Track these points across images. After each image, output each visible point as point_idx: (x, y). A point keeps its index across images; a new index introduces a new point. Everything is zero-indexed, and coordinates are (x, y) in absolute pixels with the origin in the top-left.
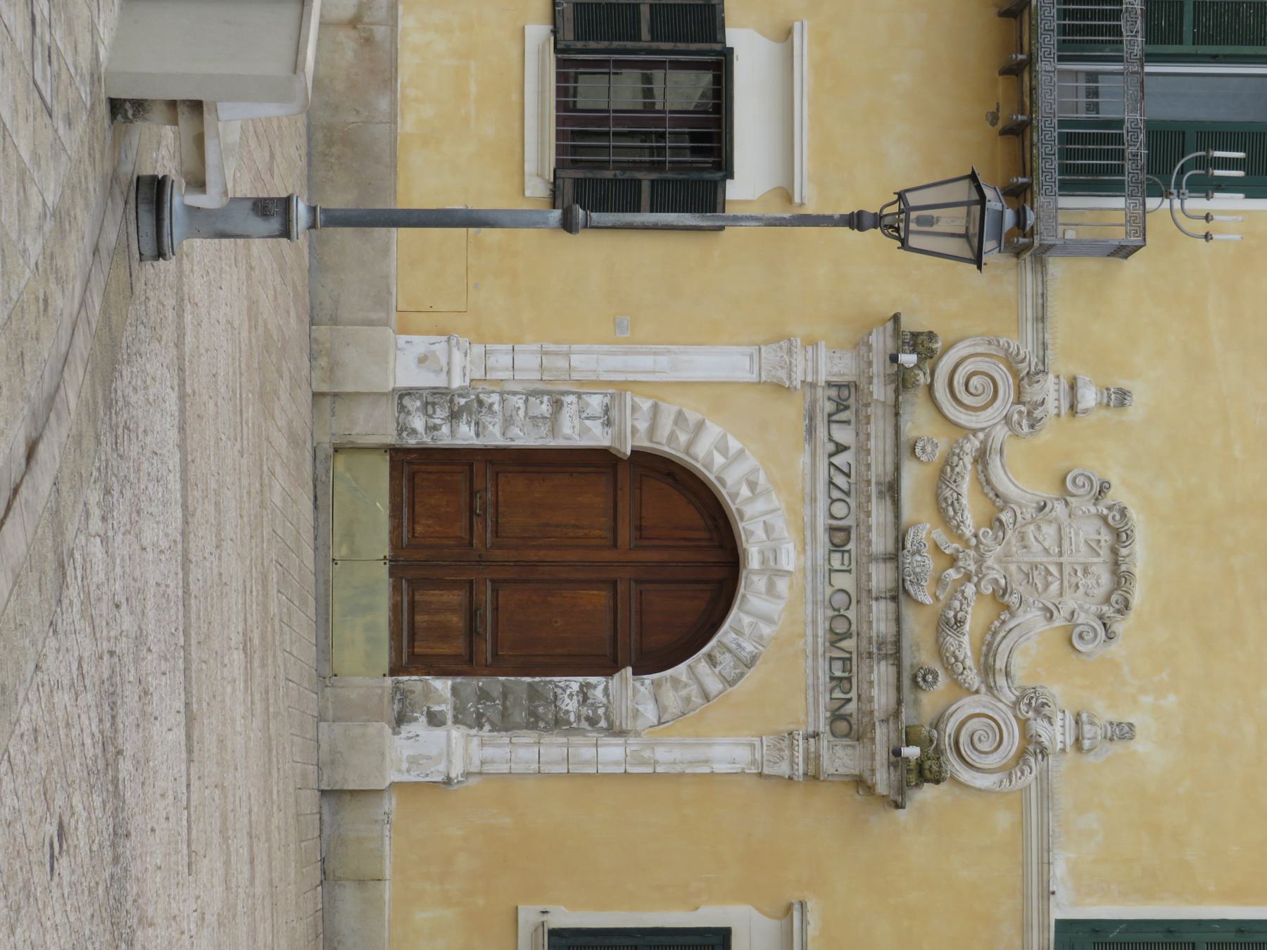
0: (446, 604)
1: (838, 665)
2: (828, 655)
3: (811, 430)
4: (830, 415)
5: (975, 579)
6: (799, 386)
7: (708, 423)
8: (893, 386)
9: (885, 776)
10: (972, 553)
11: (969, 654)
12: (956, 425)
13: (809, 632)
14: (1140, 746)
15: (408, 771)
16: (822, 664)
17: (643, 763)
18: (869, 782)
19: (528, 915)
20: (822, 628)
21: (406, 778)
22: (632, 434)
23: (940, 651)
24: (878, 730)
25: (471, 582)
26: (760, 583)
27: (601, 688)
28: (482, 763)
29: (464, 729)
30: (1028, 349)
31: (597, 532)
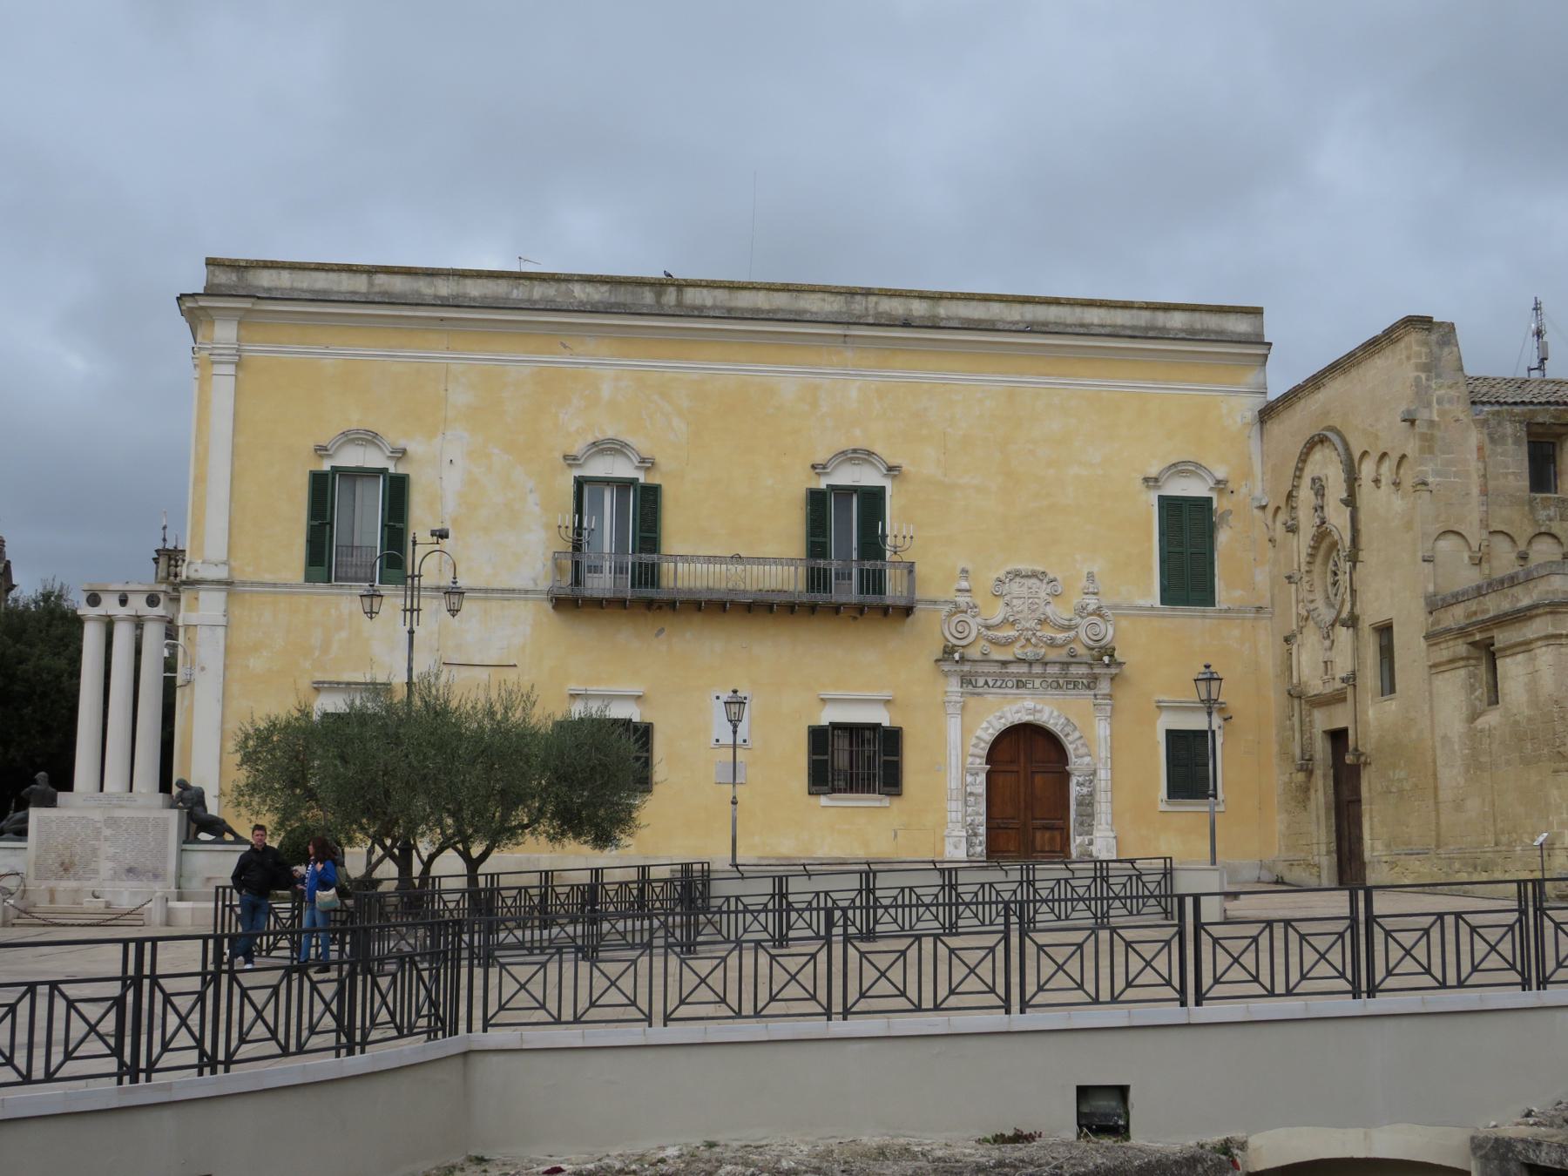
0: (1041, 838)
14: (1095, 569)
19: (1163, 807)
22: (980, 764)
23: (1061, 646)
26: (1038, 716)
30: (947, 608)
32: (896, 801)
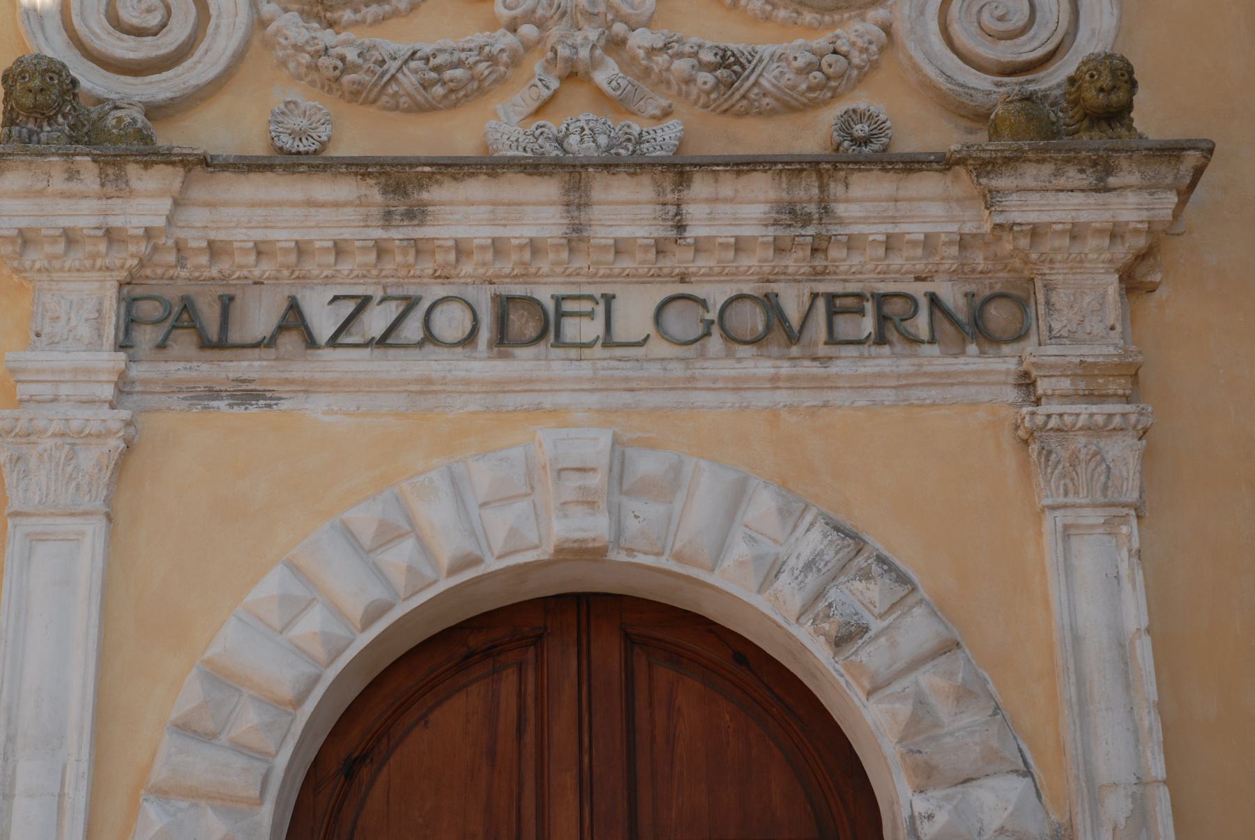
1: (845, 326)
2: (823, 350)
3: (247, 395)
4: (205, 344)
5: (619, 28)
6: (125, 414)
7: (214, 651)
8: (133, 170)
9: (1132, 198)
10: (555, 32)
11: (800, 41)
12: (239, 57)
13: (764, 399)
16: (846, 364)
18: (1141, 242)
24: (1016, 217)
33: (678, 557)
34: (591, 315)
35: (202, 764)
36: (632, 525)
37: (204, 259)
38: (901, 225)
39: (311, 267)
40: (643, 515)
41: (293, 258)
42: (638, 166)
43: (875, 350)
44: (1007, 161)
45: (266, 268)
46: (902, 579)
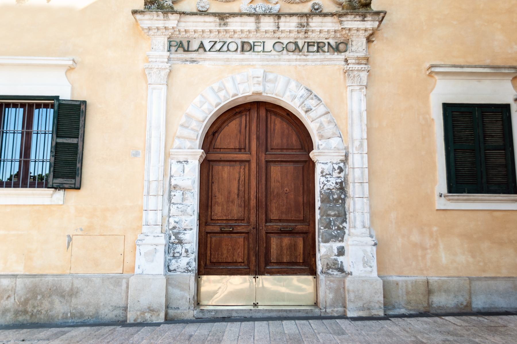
1: (311, 49)
2: (306, 53)
3: (193, 61)
4: (185, 51)
6: (169, 65)
7: (187, 111)
8: (170, 15)
9: (369, 23)
13: (294, 63)
15: (371, 267)
16: (311, 56)
17: (361, 145)
18: (371, 32)
19: (441, 204)
20: (293, 56)
21: (375, 269)
25: (267, 233)
27: (323, 166)
28: (364, 227)
29: (346, 237)
31: (242, 170)
32: (72, 194)
33: (276, 95)
34: (260, 46)
35: (186, 132)
36: (267, 88)
37: (184, 33)
38: (323, 28)
39: (205, 35)
40: (269, 86)
41: (201, 33)
42: (270, 15)
43: (317, 54)
44: (345, 15)
45: (196, 35)
46: (319, 100)
